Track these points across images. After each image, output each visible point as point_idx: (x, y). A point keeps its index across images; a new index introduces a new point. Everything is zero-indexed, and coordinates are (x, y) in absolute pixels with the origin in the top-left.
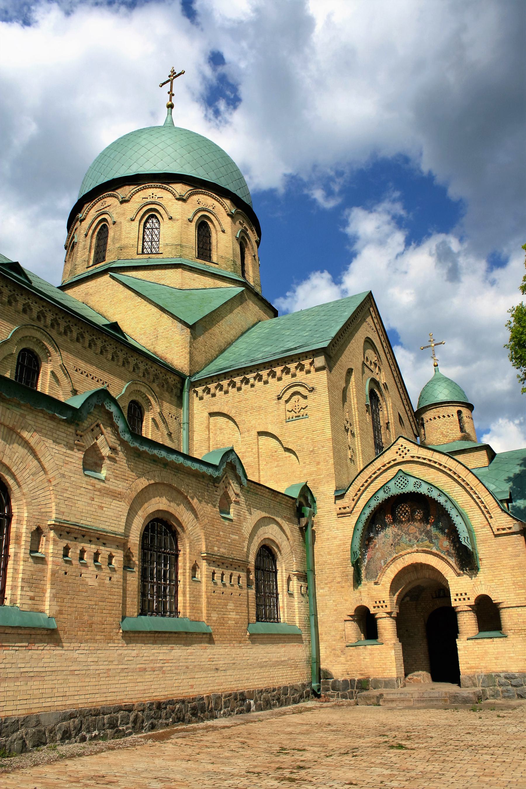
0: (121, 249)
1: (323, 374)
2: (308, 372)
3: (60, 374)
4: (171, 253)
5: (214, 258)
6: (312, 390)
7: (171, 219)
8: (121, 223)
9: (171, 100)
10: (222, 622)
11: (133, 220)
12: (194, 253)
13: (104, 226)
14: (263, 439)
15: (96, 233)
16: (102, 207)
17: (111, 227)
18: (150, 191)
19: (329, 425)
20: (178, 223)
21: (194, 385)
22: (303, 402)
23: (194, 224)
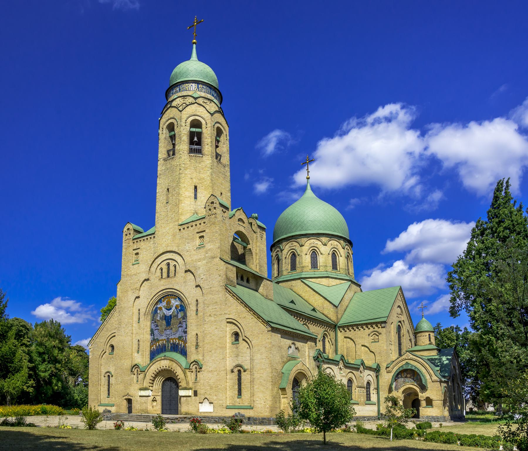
0: (303, 267)
2: (379, 328)
4: (323, 269)
5: (338, 269)
6: (380, 334)
8: (302, 255)
9: (308, 175)
10: (360, 401)
11: (306, 254)
12: (332, 268)
14: (363, 348)
15: (290, 257)
16: (292, 246)
17: (297, 256)
18: (312, 241)
20: (324, 256)
22: (377, 337)
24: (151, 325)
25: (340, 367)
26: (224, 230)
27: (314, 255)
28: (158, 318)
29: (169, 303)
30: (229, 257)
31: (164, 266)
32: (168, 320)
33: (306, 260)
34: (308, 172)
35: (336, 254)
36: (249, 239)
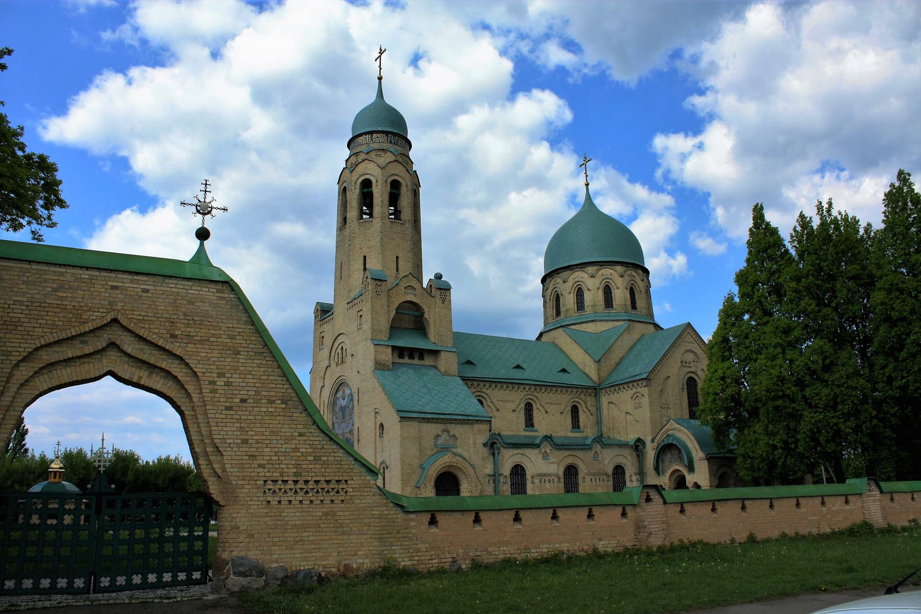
0: (567, 311)
1: (646, 389)
3: (540, 408)
5: (614, 306)
6: (643, 395)
7: (589, 290)
11: (570, 293)
12: (603, 307)
13: (558, 294)
14: (628, 416)
15: (554, 300)
18: (577, 274)
19: (648, 412)
20: (592, 292)
21: (601, 389)
23: (600, 290)
24: (332, 417)
25: (543, 450)
26: (378, 306)
27: (580, 294)
28: (337, 410)
29: (344, 392)
30: (385, 336)
31: (339, 351)
32: (343, 409)
33: (569, 301)
34: (587, 176)
35: (611, 286)
36: (424, 307)
